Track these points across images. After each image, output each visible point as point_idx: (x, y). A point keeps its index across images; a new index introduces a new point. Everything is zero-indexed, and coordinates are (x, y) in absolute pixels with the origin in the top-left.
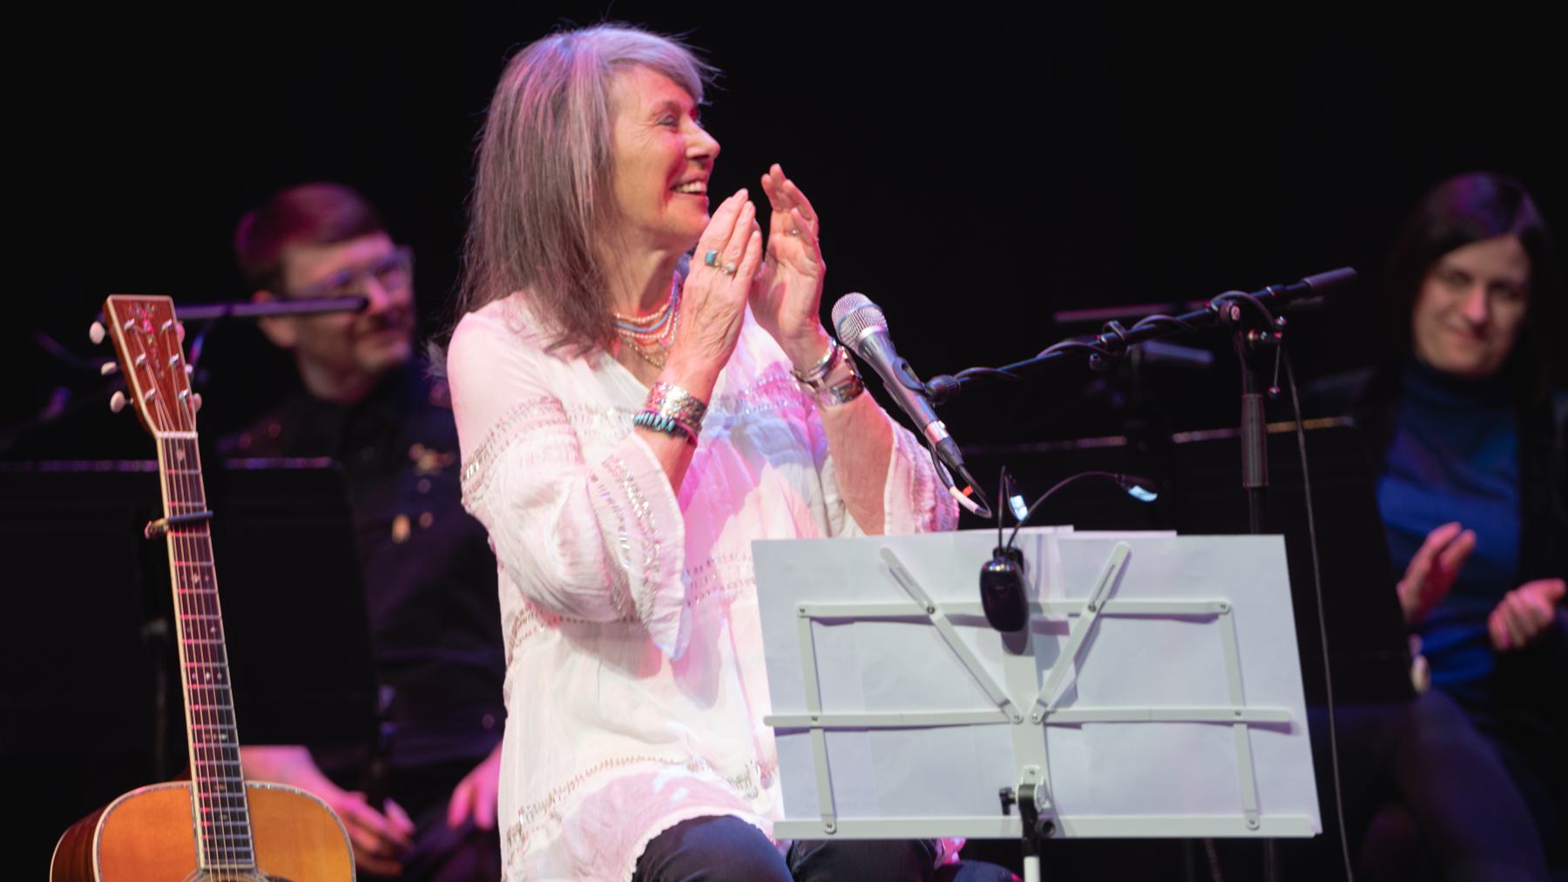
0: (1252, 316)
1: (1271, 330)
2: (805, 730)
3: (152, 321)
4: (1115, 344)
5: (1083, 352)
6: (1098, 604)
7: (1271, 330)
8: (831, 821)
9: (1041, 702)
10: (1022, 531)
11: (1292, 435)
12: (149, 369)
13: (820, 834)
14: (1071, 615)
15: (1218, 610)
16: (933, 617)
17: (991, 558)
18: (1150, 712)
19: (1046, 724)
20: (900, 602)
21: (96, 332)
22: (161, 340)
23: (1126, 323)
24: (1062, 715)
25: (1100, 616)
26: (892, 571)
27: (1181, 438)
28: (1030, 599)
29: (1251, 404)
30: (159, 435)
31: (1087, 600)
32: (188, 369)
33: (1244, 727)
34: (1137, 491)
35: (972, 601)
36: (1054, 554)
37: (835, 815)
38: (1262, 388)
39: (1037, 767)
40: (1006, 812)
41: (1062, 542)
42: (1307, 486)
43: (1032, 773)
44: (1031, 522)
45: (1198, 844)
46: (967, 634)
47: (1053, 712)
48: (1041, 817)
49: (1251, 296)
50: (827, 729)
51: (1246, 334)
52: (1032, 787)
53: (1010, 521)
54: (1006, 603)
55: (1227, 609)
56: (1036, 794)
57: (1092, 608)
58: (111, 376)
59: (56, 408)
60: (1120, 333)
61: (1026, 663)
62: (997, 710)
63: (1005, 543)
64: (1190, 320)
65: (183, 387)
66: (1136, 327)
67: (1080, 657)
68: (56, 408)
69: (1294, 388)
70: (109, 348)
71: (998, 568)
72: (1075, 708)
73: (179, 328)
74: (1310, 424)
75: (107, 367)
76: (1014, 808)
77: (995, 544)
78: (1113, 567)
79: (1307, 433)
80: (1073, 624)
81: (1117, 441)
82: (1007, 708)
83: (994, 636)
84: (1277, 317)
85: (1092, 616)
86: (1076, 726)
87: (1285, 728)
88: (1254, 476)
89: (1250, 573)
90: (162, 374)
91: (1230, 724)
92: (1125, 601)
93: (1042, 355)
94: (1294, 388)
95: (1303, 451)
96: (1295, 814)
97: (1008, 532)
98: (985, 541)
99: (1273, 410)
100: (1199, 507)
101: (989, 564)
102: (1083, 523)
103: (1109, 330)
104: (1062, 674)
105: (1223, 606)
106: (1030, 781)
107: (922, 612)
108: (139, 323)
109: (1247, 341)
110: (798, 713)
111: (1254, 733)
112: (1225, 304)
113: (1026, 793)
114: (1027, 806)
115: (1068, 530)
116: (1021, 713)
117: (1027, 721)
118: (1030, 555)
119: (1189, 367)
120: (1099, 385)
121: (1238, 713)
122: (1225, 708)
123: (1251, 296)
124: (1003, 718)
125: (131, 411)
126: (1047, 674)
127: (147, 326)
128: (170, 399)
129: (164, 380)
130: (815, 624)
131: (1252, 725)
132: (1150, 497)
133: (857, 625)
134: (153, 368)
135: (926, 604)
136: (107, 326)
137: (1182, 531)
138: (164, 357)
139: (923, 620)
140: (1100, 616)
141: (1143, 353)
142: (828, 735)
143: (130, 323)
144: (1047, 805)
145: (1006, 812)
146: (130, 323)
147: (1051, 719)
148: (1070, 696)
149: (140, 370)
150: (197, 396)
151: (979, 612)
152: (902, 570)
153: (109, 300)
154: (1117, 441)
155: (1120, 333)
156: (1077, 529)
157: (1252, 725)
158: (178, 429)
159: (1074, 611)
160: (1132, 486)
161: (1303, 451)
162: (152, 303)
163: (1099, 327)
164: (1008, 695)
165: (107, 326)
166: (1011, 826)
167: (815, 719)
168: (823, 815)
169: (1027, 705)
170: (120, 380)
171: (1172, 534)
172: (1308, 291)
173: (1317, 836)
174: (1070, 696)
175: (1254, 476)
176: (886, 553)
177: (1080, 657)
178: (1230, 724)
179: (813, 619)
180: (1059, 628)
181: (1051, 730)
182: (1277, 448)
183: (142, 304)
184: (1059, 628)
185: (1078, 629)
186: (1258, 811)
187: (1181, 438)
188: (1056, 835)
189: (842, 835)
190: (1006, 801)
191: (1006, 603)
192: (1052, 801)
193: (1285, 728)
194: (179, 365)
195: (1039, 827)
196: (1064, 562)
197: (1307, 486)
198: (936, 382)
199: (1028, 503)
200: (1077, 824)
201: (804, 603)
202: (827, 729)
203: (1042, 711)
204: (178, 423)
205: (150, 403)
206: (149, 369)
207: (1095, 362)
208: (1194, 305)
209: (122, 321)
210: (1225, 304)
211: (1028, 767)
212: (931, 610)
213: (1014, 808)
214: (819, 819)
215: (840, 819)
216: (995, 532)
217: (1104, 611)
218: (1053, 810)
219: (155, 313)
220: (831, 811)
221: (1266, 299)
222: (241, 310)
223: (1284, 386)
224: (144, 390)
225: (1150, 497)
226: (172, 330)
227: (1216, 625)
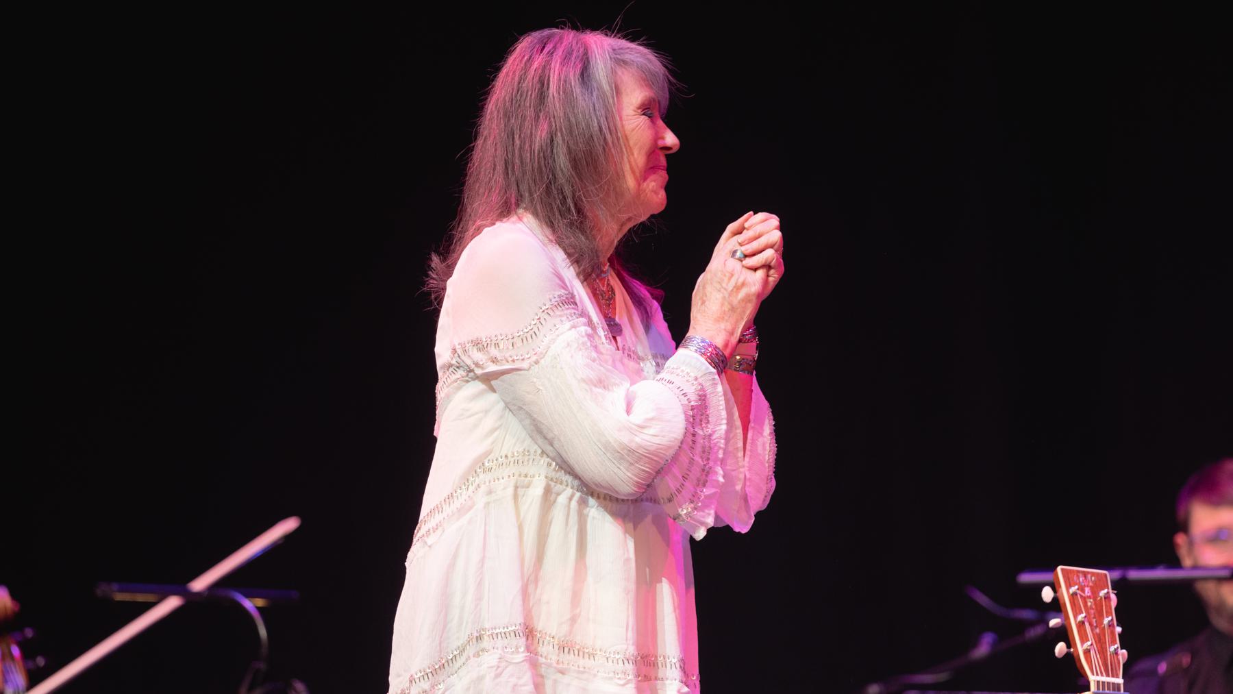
3: (1091, 588)
12: (1087, 625)
21: (1047, 594)
22: (1098, 606)
30: (1093, 679)
32: (1119, 629)
58: (1055, 629)
59: (983, 650)
65: (1114, 642)
68: (983, 650)
70: (1056, 606)
73: (1113, 597)
75: (1054, 622)
90: (1098, 630)
108: (1082, 589)
125: (1071, 659)
127: (1087, 592)
128: (1102, 651)
129: (1098, 635)
134: (1091, 624)
136: (1055, 587)
138: (1100, 616)
143: (1073, 590)
146: (1073, 590)
149: (1081, 625)
150: (1124, 651)
153: (1059, 568)
158: (1108, 675)
162: (1093, 574)
165: (1055, 587)
170: (1063, 634)
183: (1085, 574)
194: (1111, 625)
204: (1108, 670)
205: (1087, 652)
206: (1087, 625)
209: (1068, 586)
219: (1095, 583)
224: (1083, 643)
226: (1107, 597)
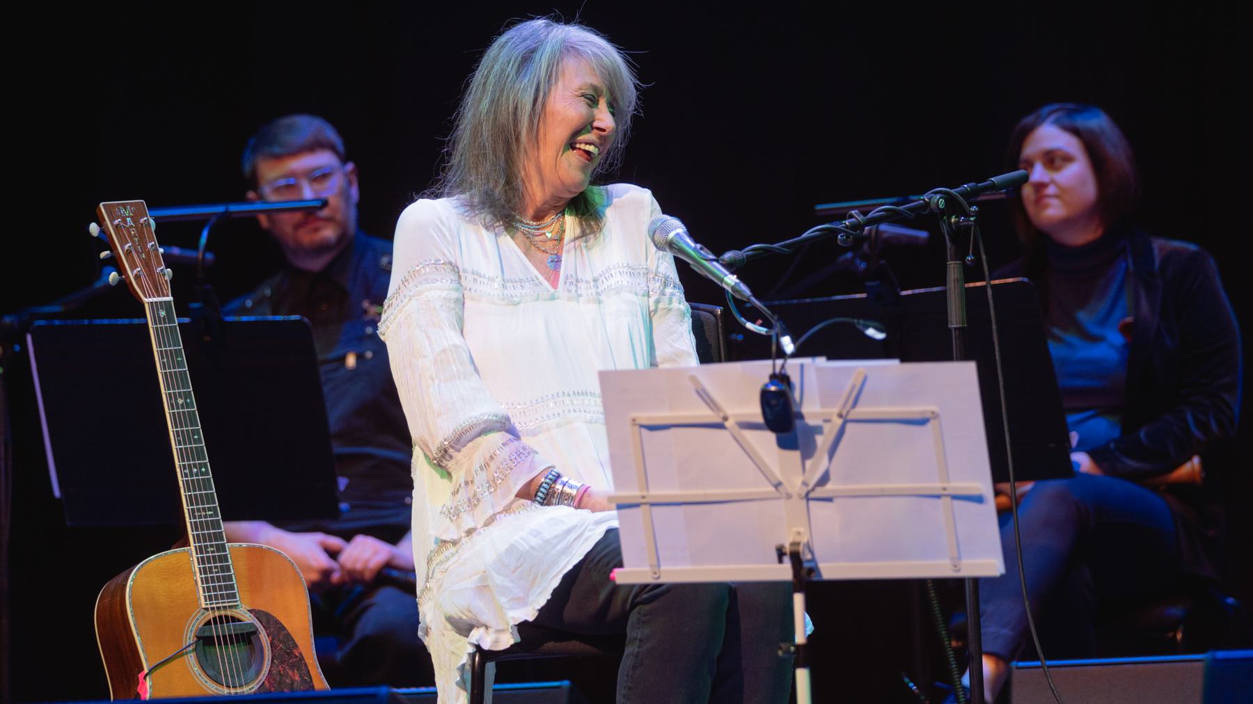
0: (953, 205)
1: (967, 215)
2: (637, 505)
4: (855, 227)
5: (835, 232)
6: (844, 413)
7: (967, 215)
8: (656, 569)
9: (805, 484)
10: (791, 362)
11: (985, 287)
13: (649, 579)
14: (827, 421)
15: (929, 415)
16: (727, 424)
17: (767, 380)
18: (882, 490)
19: (807, 498)
20: (703, 413)
23: (865, 214)
24: (820, 492)
25: (845, 422)
26: (698, 392)
27: (904, 293)
28: (795, 409)
29: (953, 270)
31: (836, 410)
33: (948, 499)
34: (871, 332)
35: (754, 411)
36: (811, 379)
37: (659, 566)
38: (960, 256)
39: (802, 530)
40: (781, 561)
41: (819, 370)
42: (994, 327)
43: (799, 533)
44: (795, 355)
45: (920, 584)
46: (749, 435)
47: (813, 490)
48: (806, 565)
49: (953, 191)
50: (653, 505)
51: (949, 218)
52: (798, 544)
53: (781, 354)
54: (780, 414)
55: (935, 416)
56: (801, 548)
57: (840, 416)
60: (861, 218)
61: (795, 455)
62: (773, 489)
63: (777, 370)
64: (910, 209)
66: (870, 215)
67: (832, 452)
69: (984, 257)
71: (773, 388)
72: (830, 486)
74: (993, 282)
76: (787, 559)
77: (770, 371)
78: (853, 387)
79: (993, 287)
80: (827, 427)
81: (864, 295)
82: (780, 488)
83: (770, 437)
84: (971, 205)
85: (839, 422)
86: (829, 500)
87: (979, 499)
88: (955, 318)
89: (951, 391)
91: (938, 497)
92: (862, 410)
93: (805, 235)
94: (984, 257)
95: (991, 302)
96: (986, 561)
97: (779, 362)
98: (759, 371)
99: (971, 273)
100: (916, 341)
101: (766, 385)
102: (834, 354)
103: (851, 216)
104: (820, 462)
105: (933, 413)
106: (798, 539)
107: (718, 420)
109: (950, 223)
110: (633, 493)
111: (957, 503)
112: (935, 198)
113: (795, 548)
114: (796, 558)
115: (821, 361)
116: (790, 490)
117: (795, 499)
118: (795, 379)
119: (912, 241)
120: (849, 255)
121: (945, 489)
122: (936, 485)
123: (953, 191)
124: (778, 495)
126: (809, 463)
130: (644, 431)
131: (955, 497)
132: (880, 336)
133: (673, 430)
135: (722, 415)
137: (904, 359)
139: (720, 426)
140: (845, 422)
141: (877, 230)
142: (654, 509)
144: (809, 557)
145: (781, 561)
147: (812, 495)
148: (824, 480)
151: (760, 420)
152: (704, 390)
154: (864, 295)
155: (861, 218)
156: (830, 358)
157: (955, 497)
159: (827, 417)
160: (868, 327)
161: (991, 302)
163: (843, 216)
164: (780, 477)
166: (784, 572)
167: (644, 497)
168: (651, 566)
169: (795, 483)
171: (894, 363)
172: (994, 187)
173: (1002, 576)
174: (824, 480)
175: (955, 318)
176: (693, 379)
177: (832, 452)
178: (938, 497)
179: (641, 426)
180: (818, 430)
181: (812, 503)
182: (974, 300)
184: (818, 430)
185: (830, 431)
186: (960, 558)
187: (904, 293)
188: (814, 578)
189: (666, 579)
190: (781, 554)
191: (780, 414)
192: (811, 552)
193: (979, 499)
195: (804, 573)
196: (820, 382)
197: (994, 327)
198: (728, 256)
199: (794, 341)
200: (830, 570)
201: (635, 415)
202: (653, 505)
203: (805, 490)
207: (843, 241)
208: (915, 198)
210: (935, 198)
211: (795, 529)
212: (726, 419)
213: (787, 559)
214: (648, 569)
215: (663, 568)
216: (770, 362)
217: (850, 417)
218: (813, 560)
220: (655, 562)
221: (965, 194)
222: (234, 208)
223: (976, 253)
225: (880, 336)
227: (929, 426)
